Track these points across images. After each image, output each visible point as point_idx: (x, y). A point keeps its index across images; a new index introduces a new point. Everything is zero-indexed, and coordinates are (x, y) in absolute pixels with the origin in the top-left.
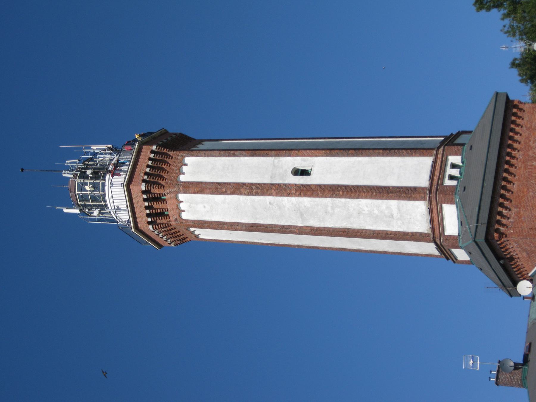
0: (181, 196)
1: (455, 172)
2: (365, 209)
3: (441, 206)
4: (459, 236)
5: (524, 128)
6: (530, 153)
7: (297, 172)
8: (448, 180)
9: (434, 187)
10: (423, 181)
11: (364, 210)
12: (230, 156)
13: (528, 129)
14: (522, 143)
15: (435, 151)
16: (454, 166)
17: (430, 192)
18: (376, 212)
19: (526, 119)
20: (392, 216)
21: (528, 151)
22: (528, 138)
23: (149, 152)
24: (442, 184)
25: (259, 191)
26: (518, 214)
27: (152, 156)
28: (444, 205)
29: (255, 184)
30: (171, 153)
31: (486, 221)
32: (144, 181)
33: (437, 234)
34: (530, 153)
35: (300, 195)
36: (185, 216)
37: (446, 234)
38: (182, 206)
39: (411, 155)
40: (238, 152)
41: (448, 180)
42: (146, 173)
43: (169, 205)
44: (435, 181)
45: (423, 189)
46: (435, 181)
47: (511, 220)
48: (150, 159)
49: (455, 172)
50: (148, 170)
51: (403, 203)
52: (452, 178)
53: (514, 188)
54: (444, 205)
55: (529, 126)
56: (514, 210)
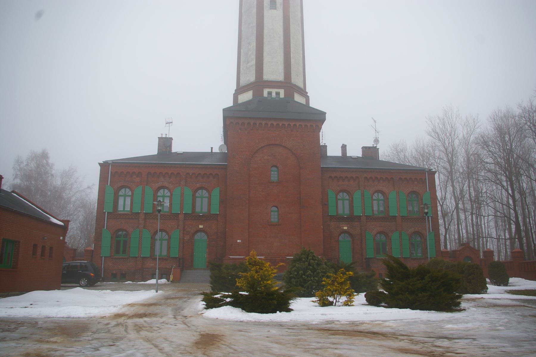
1: (274, 95)
2: (252, 46)
3: (251, 90)
8: (268, 92)
10: (267, 76)
11: (250, 46)
16: (278, 94)
18: (250, 53)
20: (248, 63)
24: (264, 88)
28: (252, 91)
35: (257, 5)
41: (268, 92)
49: (274, 95)
51: (254, 67)
52: (270, 93)
54: (252, 91)
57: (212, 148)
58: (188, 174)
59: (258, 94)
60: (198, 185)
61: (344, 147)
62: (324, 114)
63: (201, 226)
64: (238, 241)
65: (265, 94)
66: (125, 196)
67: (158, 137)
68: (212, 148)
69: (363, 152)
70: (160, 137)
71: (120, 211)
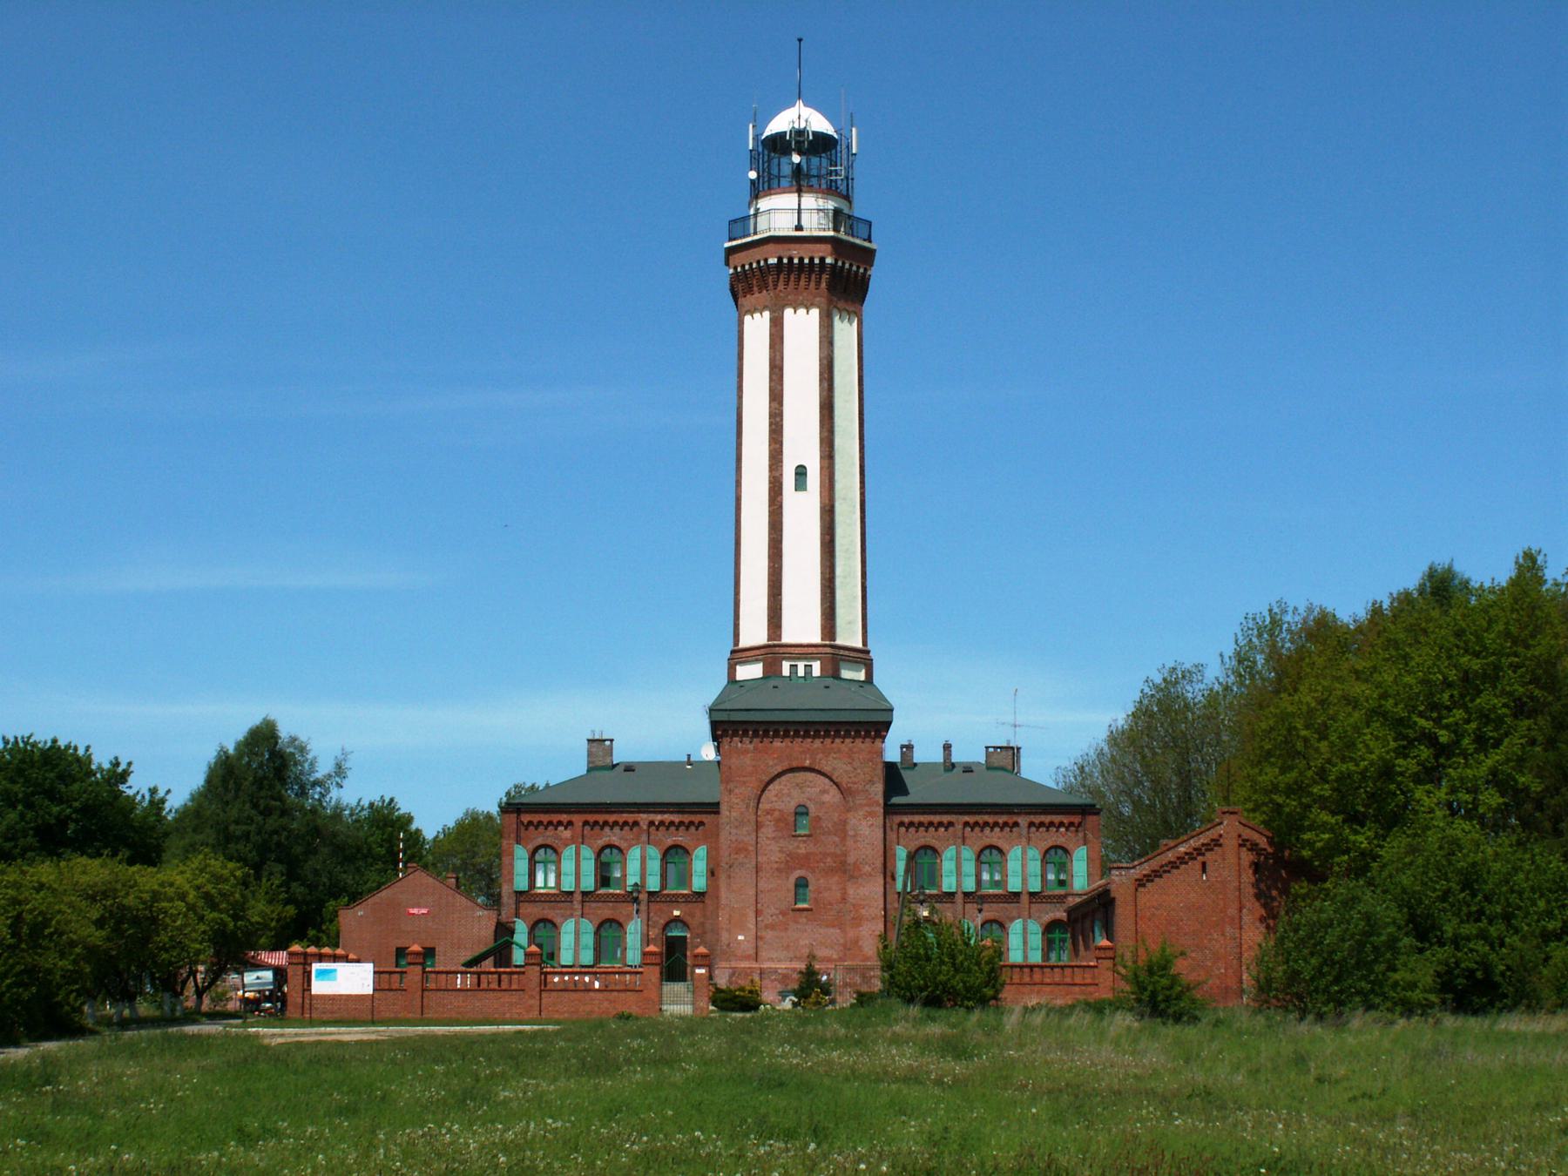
0: (767, 314)
1: (801, 672)
3: (757, 661)
4: (737, 682)
5: (851, 745)
6: (820, 756)
7: (801, 472)
9: (782, 650)
12: (821, 374)
13: (850, 750)
14: (834, 745)
15: (827, 642)
17: (775, 646)
19: (863, 746)
21: (823, 753)
22: (839, 751)
23: (821, 254)
24: (784, 659)
25: (773, 427)
26: (746, 752)
27: (817, 261)
29: (782, 420)
30: (823, 285)
31: (732, 719)
32: (780, 259)
33: (740, 655)
34: (820, 756)
36: (747, 318)
37: (738, 667)
38: (757, 315)
39: (823, 614)
40: (826, 385)
42: (791, 259)
43: (757, 297)
44: (789, 650)
45: (780, 638)
46: (789, 650)
47: (739, 744)
48: (812, 259)
49: (801, 672)
50: (796, 261)
53: (777, 743)
55: (855, 750)
56: (751, 747)
57: (689, 756)
58: (651, 823)
59: (772, 670)
60: (670, 841)
61: (947, 748)
62: (892, 710)
63: (676, 913)
64: (741, 938)
65: (786, 671)
66: (545, 863)
67: (589, 740)
68: (689, 756)
69: (988, 755)
70: (591, 738)
71: (540, 888)
